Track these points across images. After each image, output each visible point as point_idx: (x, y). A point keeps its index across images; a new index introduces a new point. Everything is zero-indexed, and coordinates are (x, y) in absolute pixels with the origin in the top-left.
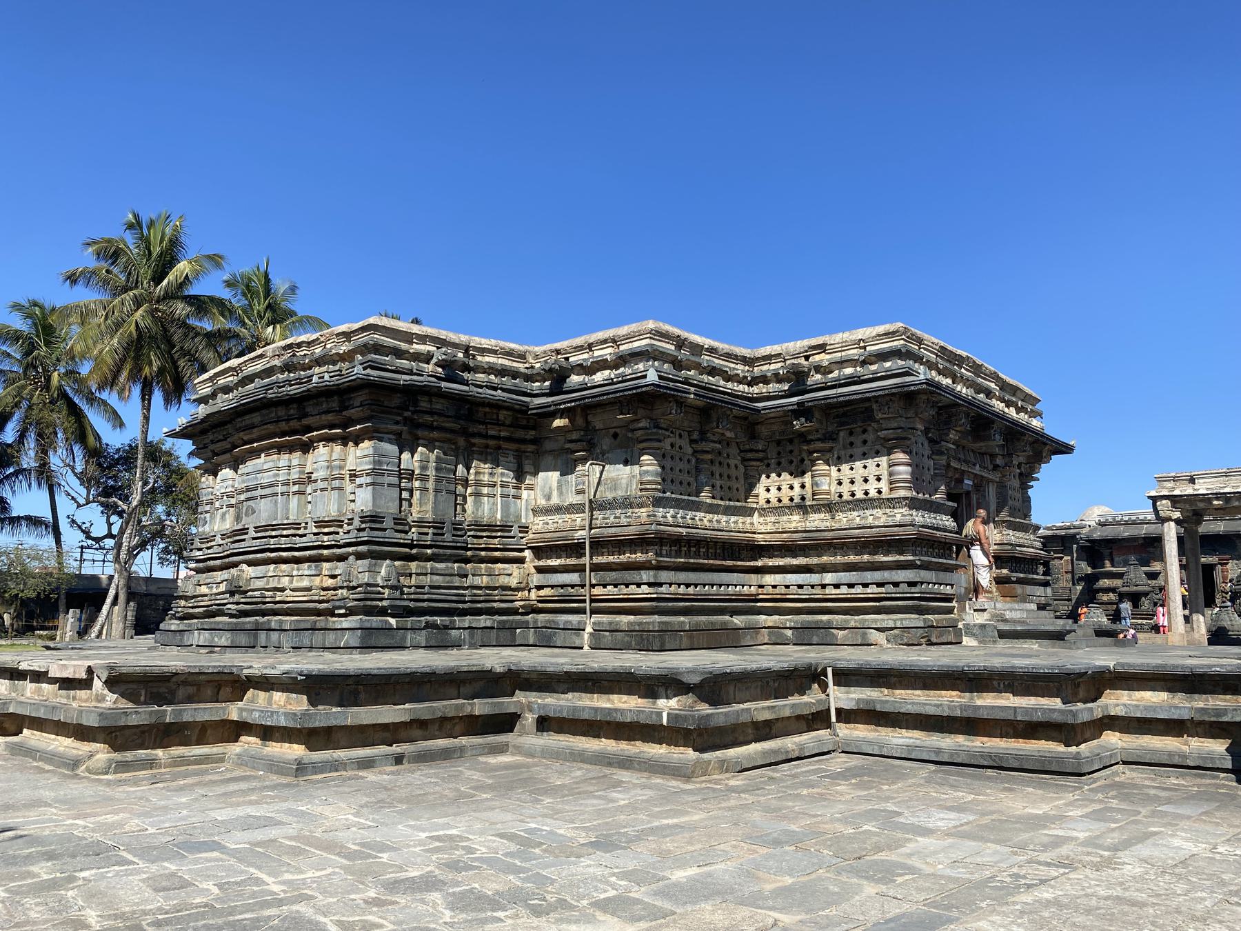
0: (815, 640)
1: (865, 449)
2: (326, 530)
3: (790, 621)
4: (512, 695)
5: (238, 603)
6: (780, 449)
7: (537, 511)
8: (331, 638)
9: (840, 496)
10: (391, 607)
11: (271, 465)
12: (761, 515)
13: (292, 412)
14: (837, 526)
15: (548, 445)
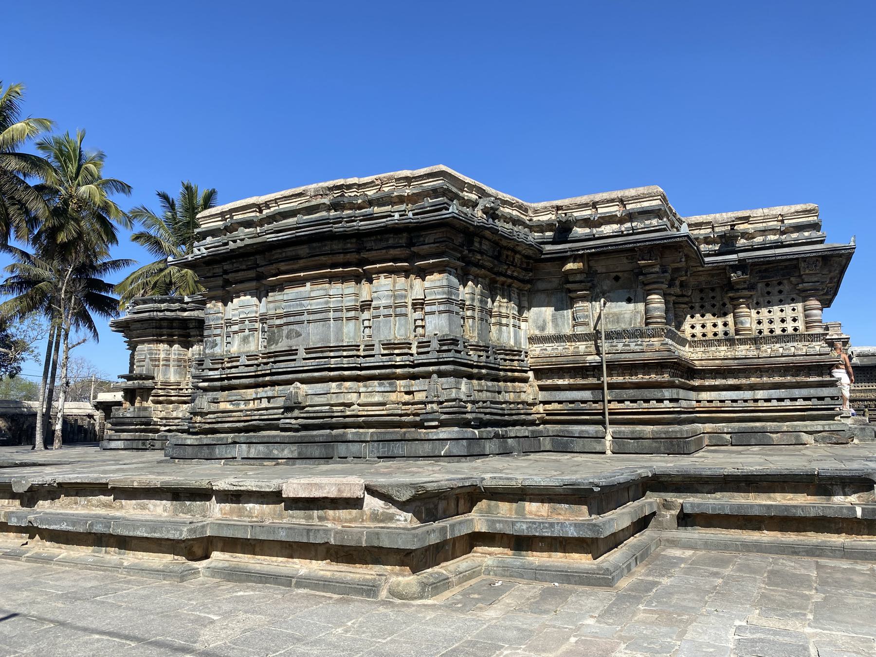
0: (753, 442)
1: (782, 297)
2: (397, 351)
3: (728, 427)
4: (643, 495)
5: (296, 418)
6: (703, 295)
7: (532, 340)
8: (427, 448)
9: (760, 332)
10: (474, 419)
11: (322, 293)
12: (690, 346)
13: (349, 245)
14: (764, 355)
15: (541, 285)
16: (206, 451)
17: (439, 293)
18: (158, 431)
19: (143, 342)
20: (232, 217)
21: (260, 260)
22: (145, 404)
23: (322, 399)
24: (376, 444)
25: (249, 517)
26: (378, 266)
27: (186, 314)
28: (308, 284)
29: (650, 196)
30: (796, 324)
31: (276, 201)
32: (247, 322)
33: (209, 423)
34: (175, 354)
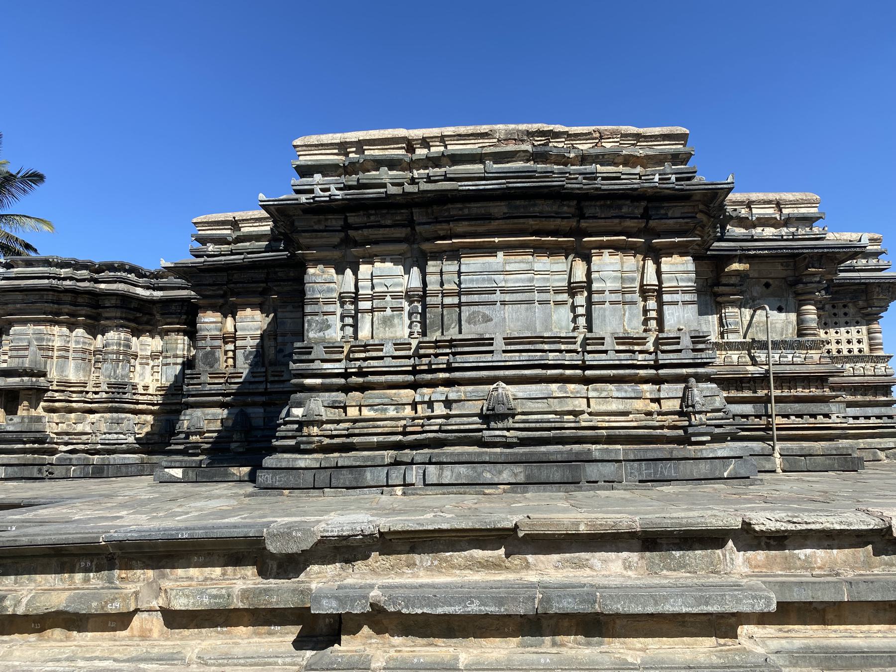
1: (847, 319)
2: (636, 348)
5: (508, 430)
8: (703, 469)
11: (524, 266)
16: (346, 477)
17: (682, 280)
18: (53, 452)
19: (24, 322)
20: (361, 151)
21: (418, 215)
22: (33, 413)
23: (540, 405)
24: (636, 464)
25: (806, 569)
26: (605, 239)
27: (103, 286)
28: (500, 254)
29: (809, 203)
30: (861, 346)
31: (442, 139)
32: (388, 298)
33: (332, 437)
34: (77, 342)
